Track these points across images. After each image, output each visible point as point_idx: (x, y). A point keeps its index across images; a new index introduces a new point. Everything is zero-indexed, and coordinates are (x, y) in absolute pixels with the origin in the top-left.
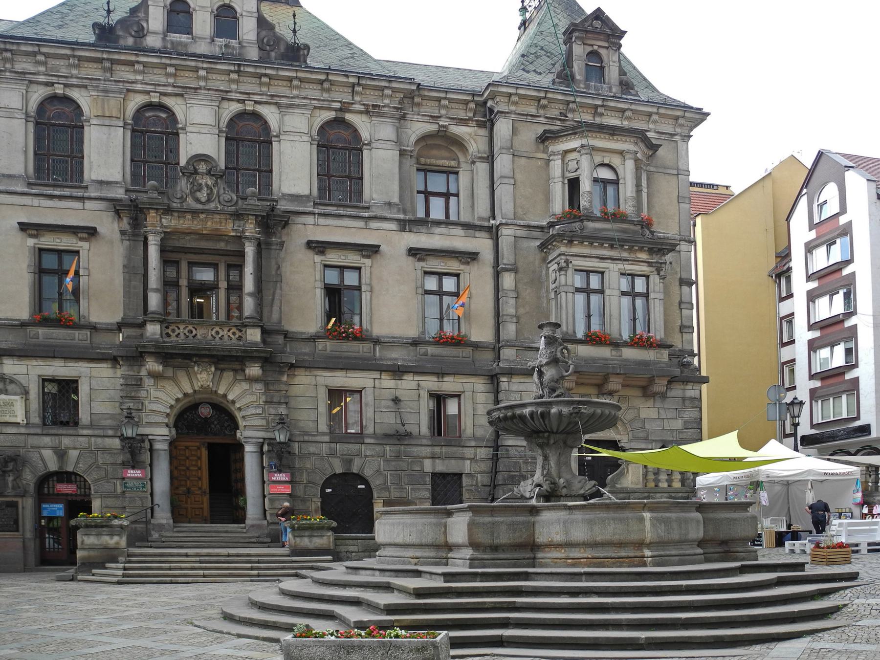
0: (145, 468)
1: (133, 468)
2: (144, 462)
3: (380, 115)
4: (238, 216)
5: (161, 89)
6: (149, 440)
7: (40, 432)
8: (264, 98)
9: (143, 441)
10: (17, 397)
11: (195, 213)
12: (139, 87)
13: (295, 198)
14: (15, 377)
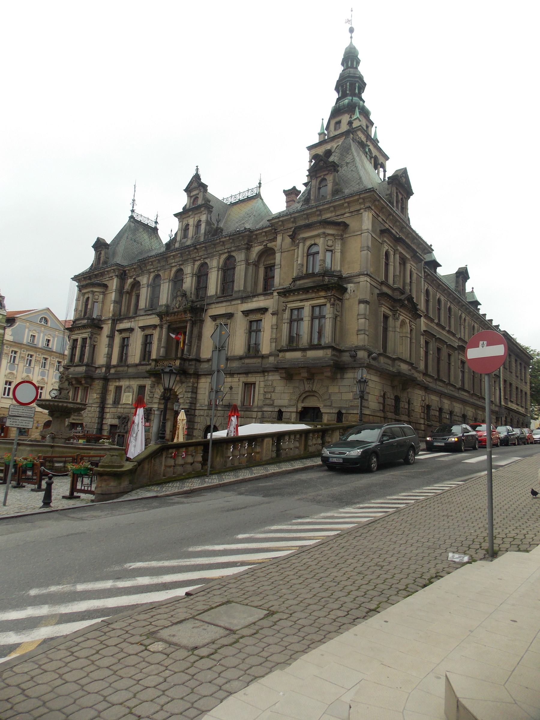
3: (239, 250)
4: (185, 312)
5: (178, 263)
8: (206, 256)
9: (151, 410)
11: (174, 313)
12: (173, 265)
13: (211, 297)
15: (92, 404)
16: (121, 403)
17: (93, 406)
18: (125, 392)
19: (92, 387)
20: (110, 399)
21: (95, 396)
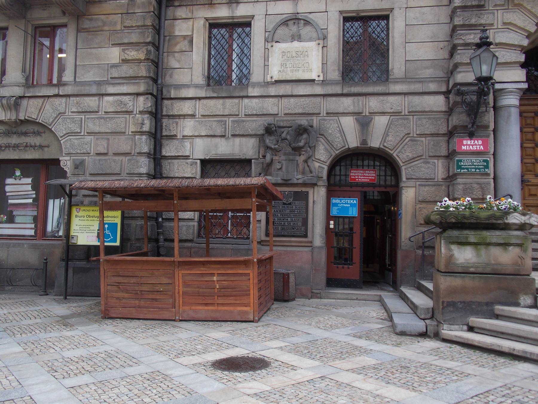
0: (488, 136)
1: (471, 135)
2: (487, 127)
6: (496, 91)
7: (339, 92)
10: (312, 45)
14: (311, 16)
15: (99, 83)
16: (256, 76)
17: (111, 90)
18: (271, 38)
19: (86, 24)
20: (189, 67)
21: (114, 54)
